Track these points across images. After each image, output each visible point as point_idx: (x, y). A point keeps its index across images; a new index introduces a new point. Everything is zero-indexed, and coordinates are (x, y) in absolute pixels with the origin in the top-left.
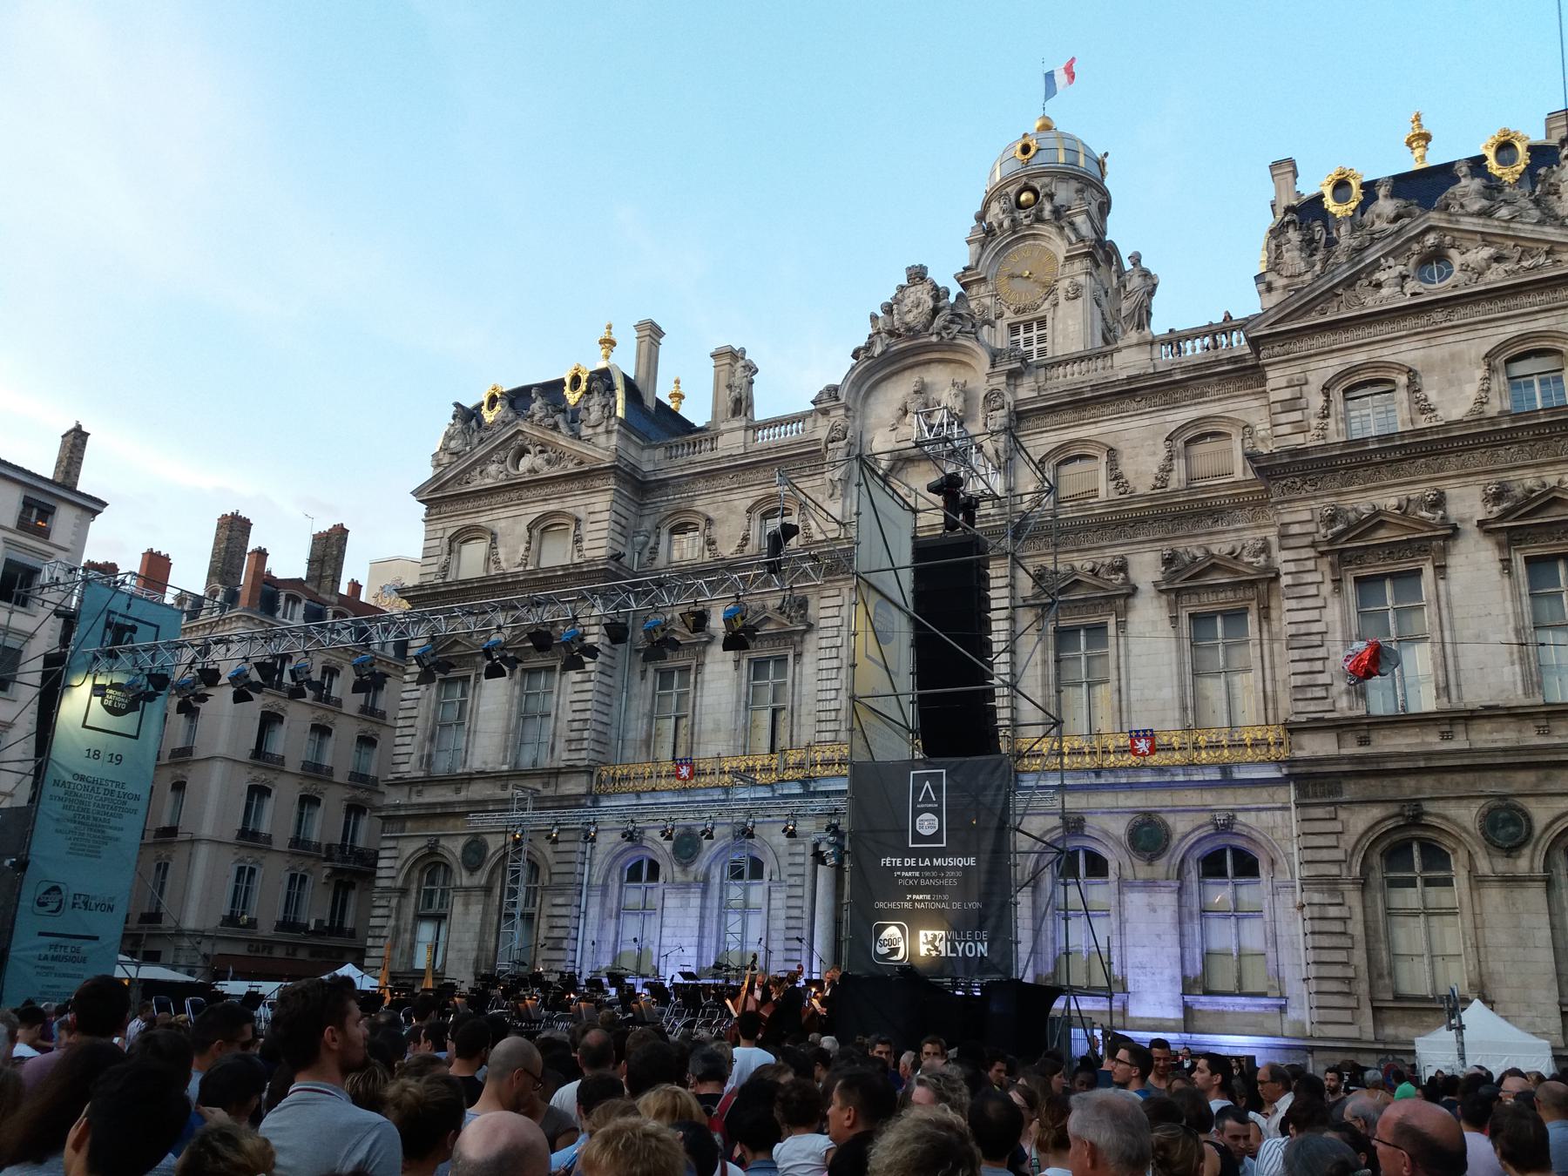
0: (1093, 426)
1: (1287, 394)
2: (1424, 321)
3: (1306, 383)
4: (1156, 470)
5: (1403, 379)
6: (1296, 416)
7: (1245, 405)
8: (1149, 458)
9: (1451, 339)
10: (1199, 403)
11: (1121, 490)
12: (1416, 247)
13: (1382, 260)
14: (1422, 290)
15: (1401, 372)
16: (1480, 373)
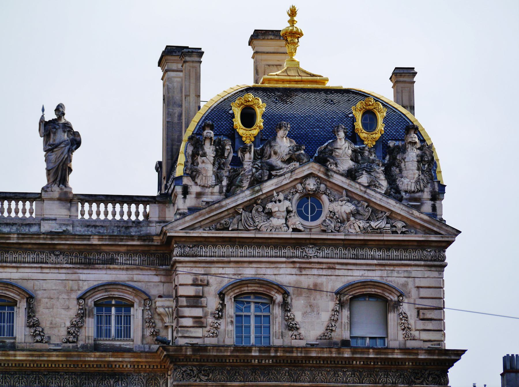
0: (15, 270)
1: (191, 291)
2: (298, 253)
3: (208, 284)
4: (68, 324)
5: (279, 298)
6: (198, 312)
7: (146, 278)
8: (63, 312)
9: (315, 272)
10: (110, 268)
11: (38, 338)
12: (300, 187)
13: (275, 194)
14: (301, 228)
15: (278, 292)
16: (331, 304)
